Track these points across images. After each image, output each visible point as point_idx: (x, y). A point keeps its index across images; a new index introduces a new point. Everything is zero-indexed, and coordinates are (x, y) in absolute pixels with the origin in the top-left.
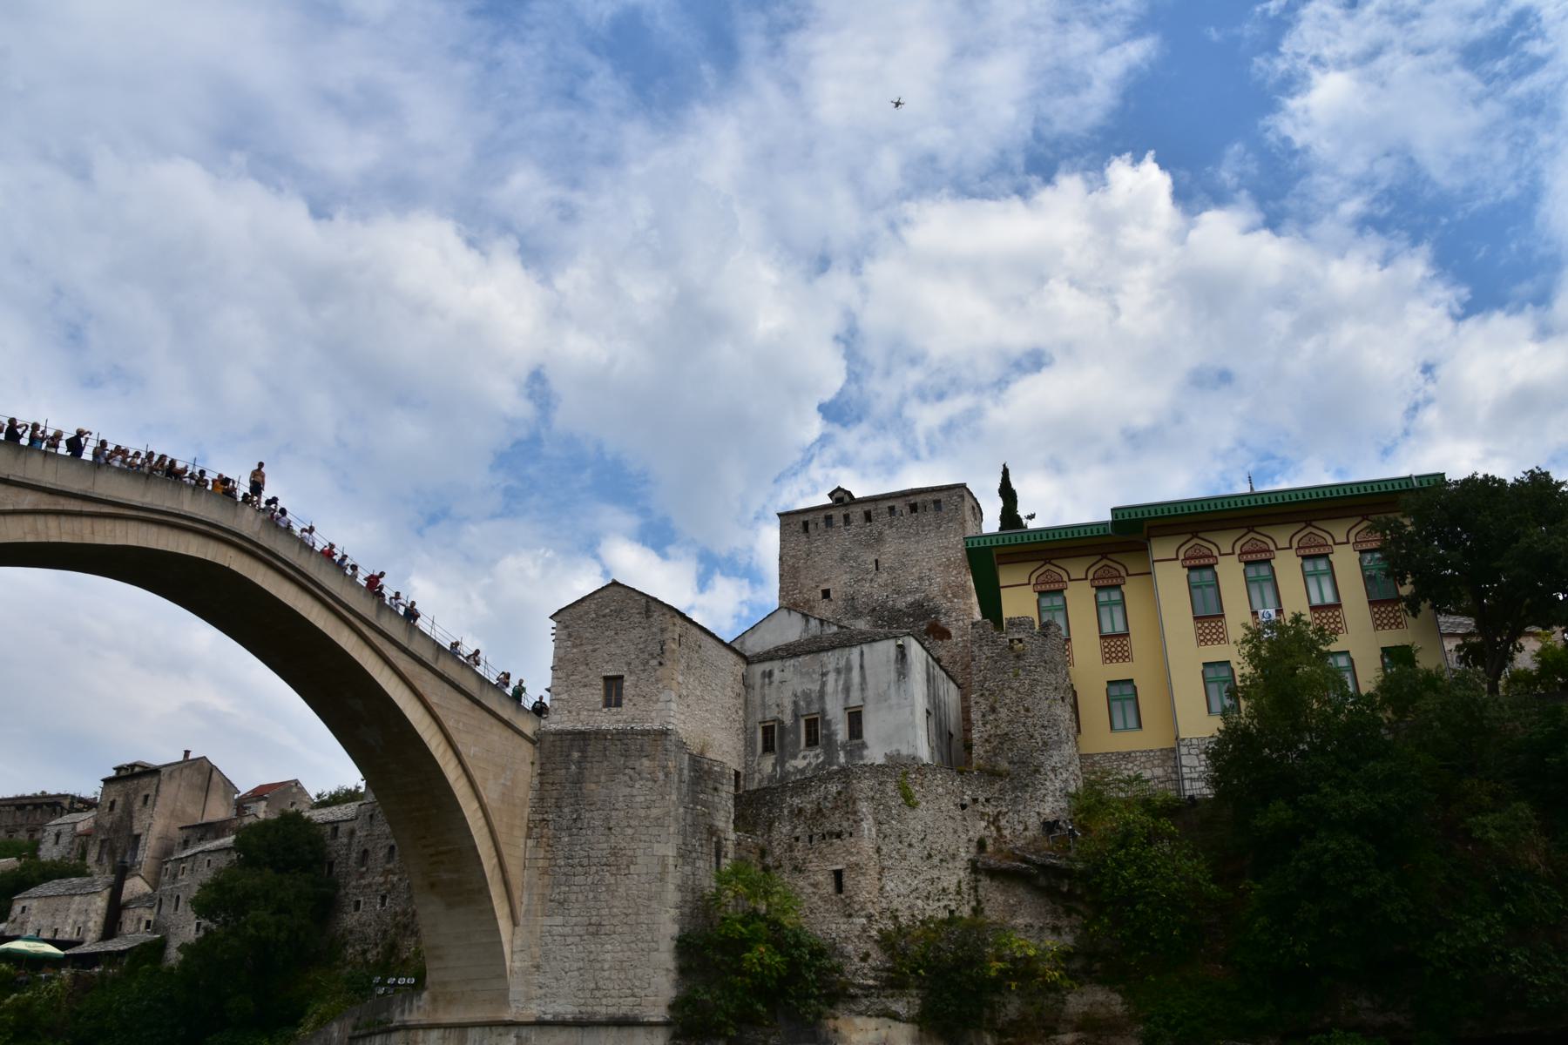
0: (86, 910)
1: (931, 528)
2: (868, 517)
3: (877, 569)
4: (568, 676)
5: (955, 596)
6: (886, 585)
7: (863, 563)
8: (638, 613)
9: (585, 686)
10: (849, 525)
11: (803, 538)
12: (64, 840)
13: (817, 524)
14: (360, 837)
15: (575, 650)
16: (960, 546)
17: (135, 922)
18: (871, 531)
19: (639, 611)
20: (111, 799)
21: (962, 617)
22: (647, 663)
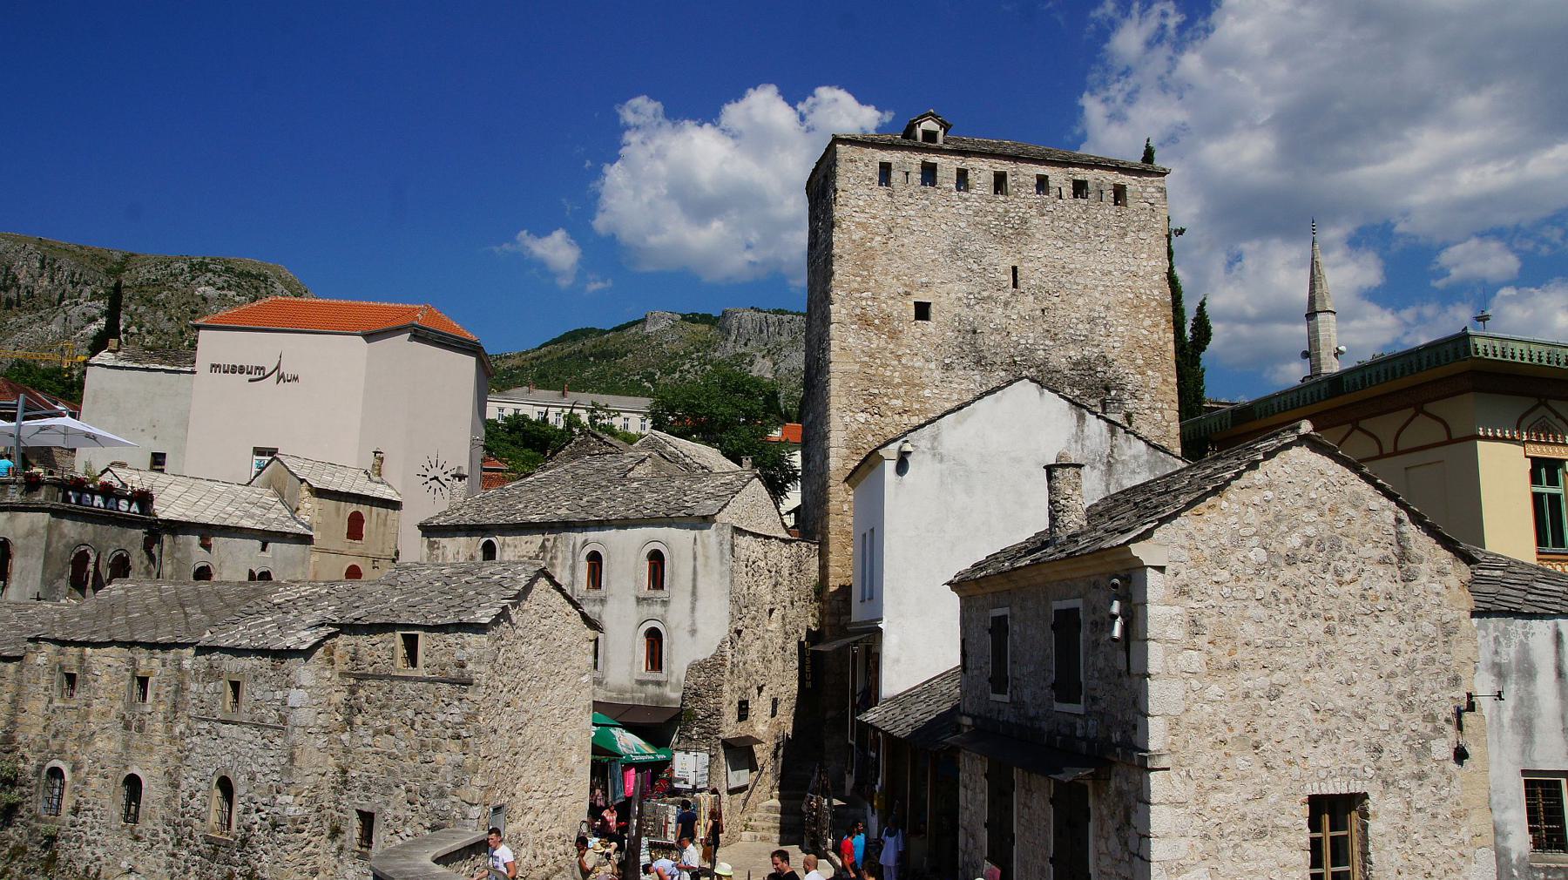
1: (1109, 232)
2: (1000, 182)
3: (1015, 285)
4: (1202, 794)
5: (1148, 365)
6: (1033, 319)
7: (991, 269)
8: (1383, 561)
9: (1261, 834)
10: (967, 189)
11: (881, 193)
13: (907, 173)
15: (1215, 689)
16: (1156, 278)
18: (1007, 211)
19: (1378, 553)
21: (1159, 405)
22: (1426, 748)
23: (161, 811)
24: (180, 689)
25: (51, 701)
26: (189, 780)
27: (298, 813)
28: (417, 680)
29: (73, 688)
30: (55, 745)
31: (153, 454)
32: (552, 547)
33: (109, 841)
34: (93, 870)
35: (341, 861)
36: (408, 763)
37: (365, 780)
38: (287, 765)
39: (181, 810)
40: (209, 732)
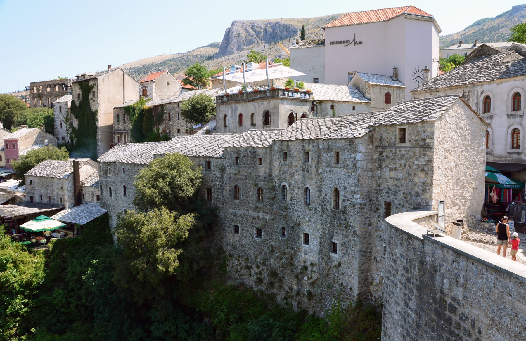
0: (62, 188)
12: (64, 110)
14: (230, 174)
17: (91, 196)
20: (78, 93)
23: (317, 200)
24: (319, 156)
25: (280, 162)
26: (325, 189)
27: (362, 202)
28: (406, 147)
29: (286, 158)
30: (283, 177)
31: (314, 79)
32: (467, 96)
33: (302, 210)
34: (298, 220)
35: (379, 221)
36: (403, 182)
37: (387, 189)
38: (357, 183)
39: (323, 200)
40: (330, 171)
